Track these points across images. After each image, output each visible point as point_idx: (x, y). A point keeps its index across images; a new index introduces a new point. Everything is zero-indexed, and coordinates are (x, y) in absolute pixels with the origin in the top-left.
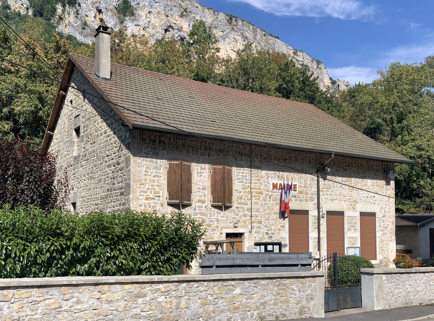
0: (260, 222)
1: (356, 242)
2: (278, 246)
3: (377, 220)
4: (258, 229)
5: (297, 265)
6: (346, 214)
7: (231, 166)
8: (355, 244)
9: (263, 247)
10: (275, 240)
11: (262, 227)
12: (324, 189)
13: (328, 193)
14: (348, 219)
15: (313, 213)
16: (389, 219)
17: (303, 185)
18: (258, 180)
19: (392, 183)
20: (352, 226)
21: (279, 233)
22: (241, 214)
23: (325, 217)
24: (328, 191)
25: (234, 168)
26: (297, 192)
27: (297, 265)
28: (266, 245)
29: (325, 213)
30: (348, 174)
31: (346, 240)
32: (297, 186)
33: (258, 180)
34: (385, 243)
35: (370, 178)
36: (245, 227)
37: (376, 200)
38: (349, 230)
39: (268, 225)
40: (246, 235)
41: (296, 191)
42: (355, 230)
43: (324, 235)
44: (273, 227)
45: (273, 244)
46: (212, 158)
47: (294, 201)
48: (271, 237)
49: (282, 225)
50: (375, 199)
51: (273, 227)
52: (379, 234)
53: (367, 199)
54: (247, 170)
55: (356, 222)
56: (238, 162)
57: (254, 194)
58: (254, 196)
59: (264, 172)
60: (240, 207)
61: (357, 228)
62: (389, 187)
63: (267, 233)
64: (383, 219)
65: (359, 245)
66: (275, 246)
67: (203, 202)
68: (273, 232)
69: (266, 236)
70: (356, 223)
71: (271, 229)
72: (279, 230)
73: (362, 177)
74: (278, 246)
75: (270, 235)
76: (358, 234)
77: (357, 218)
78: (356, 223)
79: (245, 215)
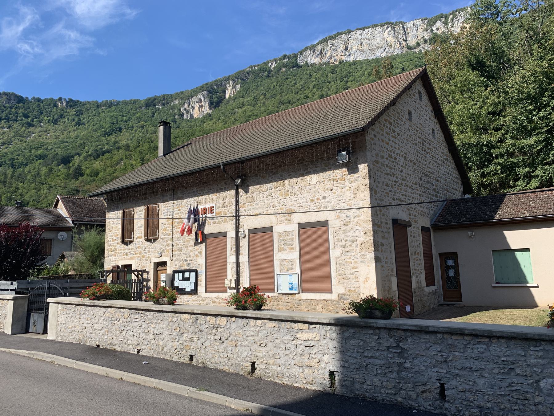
0: (180, 250)
1: (294, 266)
2: (194, 273)
3: (331, 230)
4: (178, 257)
5: (8, 290)
6: (276, 230)
7: (157, 202)
8: (292, 269)
9: (181, 274)
10: (192, 267)
11: (182, 255)
12: (247, 204)
13: (251, 207)
14: (280, 236)
15: (231, 234)
16: (357, 227)
17: (221, 205)
18: (179, 210)
19: (363, 168)
20: (286, 244)
21: (197, 260)
22: (165, 244)
23: (247, 237)
24: (251, 205)
25: (161, 204)
26: (215, 214)
27: (8, 290)
28: (183, 272)
29: (247, 232)
30: (279, 177)
31: (277, 264)
32: (214, 208)
33: (179, 210)
34: (350, 266)
35: (315, 172)
36: (168, 256)
37: (328, 202)
38: (281, 250)
39: (187, 252)
40: (168, 264)
41: (213, 213)
42: (291, 249)
43: (244, 259)
44: (191, 254)
45: (190, 271)
46: (147, 200)
47: (212, 224)
48: (189, 264)
49: (199, 250)
50: (327, 200)
51: (191, 254)
52: (335, 253)
53: (312, 203)
54: (170, 203)
55: (293, 239)
56: (164, 198)
57: (176, 224)
58: (176, 226)
59: (185, 200)
60: (165, 238)
61: (294, 246)
62: (356, 175)
63: (186, 260)
64: (344, 228)
65: (298, 271)
66: (191, 273)
67: (141, 238)
68: (191, 259)
69: (185, 263)
70: (291, 240)
71: (190, 256)
72: (197, 256)
73: (302, 175)
74: (194, 273)
75: (189, 262)
76: (295, 255)
77: (294, 233)
78: (291, 240)
79: (168, 245)
